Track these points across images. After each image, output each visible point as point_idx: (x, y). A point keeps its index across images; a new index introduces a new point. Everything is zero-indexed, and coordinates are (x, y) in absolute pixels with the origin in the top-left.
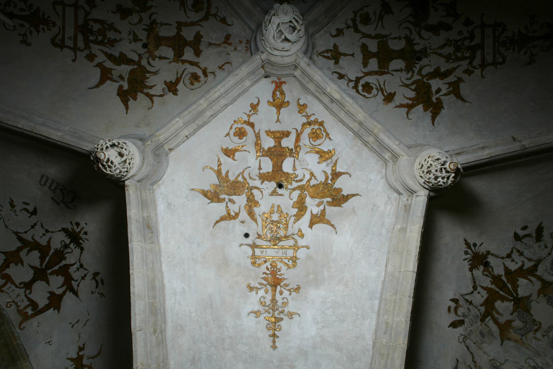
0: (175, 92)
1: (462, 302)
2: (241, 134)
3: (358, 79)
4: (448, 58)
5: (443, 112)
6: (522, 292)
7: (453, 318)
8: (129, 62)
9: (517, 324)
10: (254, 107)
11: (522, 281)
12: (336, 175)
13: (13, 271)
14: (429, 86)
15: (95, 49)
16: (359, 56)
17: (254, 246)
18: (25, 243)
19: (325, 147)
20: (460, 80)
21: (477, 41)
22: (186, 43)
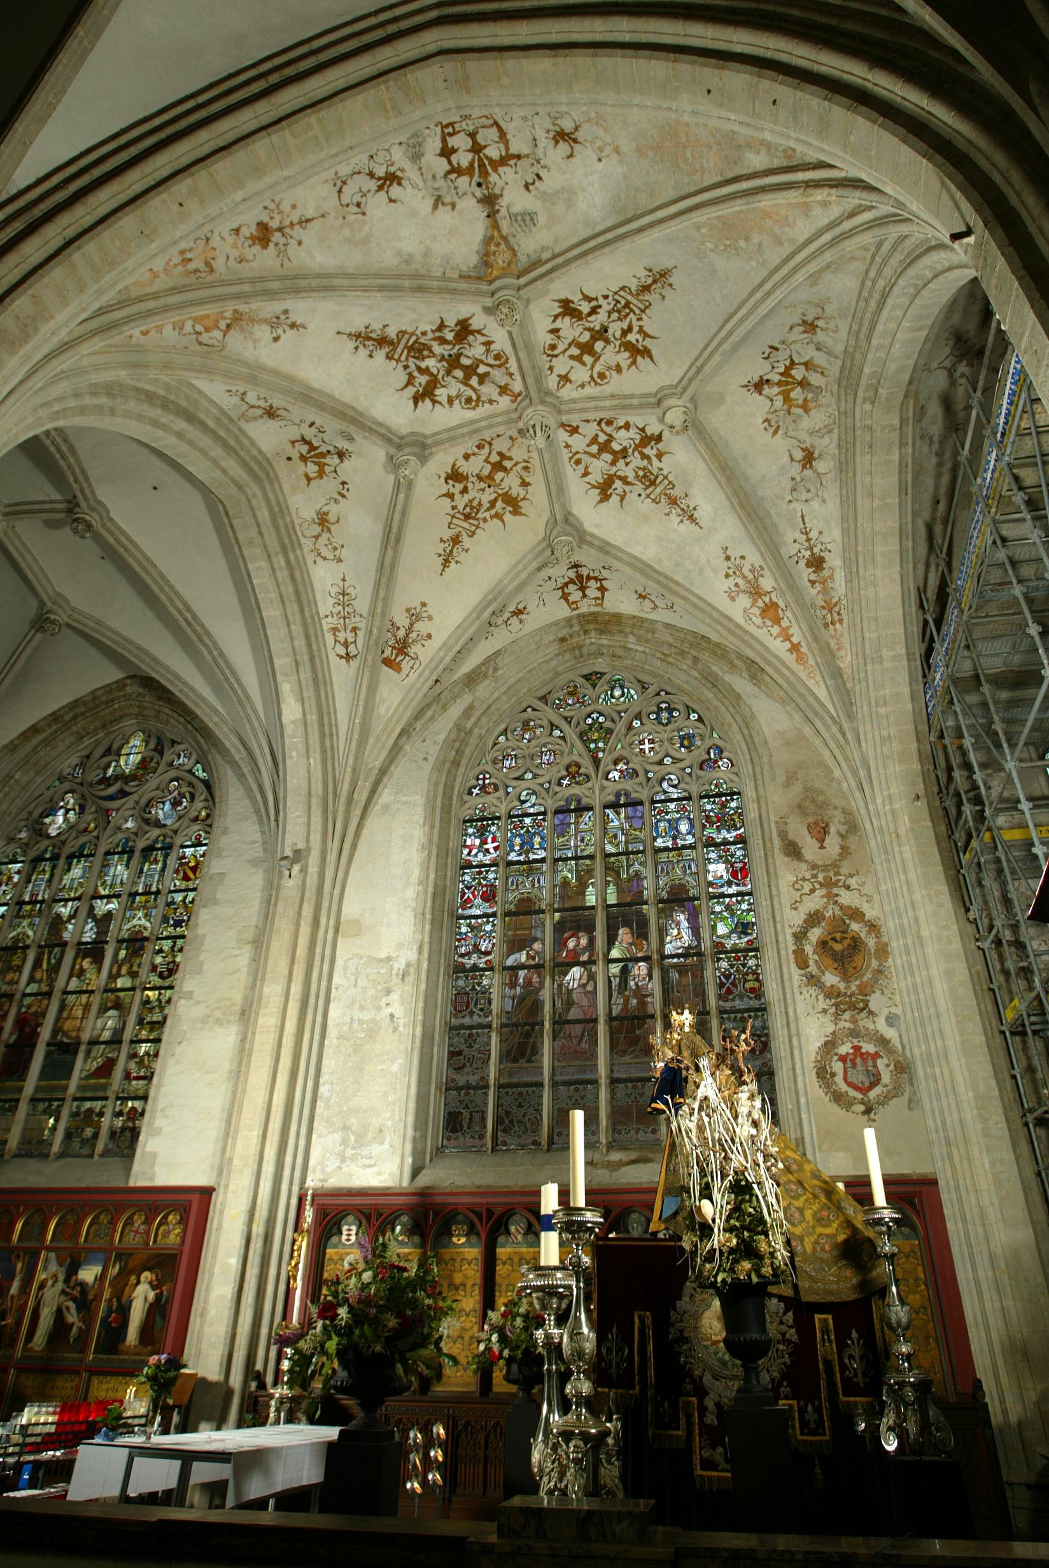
0: (529, 484)
1: (770, 416)
2: (578, 462)
3: (592, 377)
4: (619, 319)
5: (653, 352)
6: (799, 378)
7: (771, 430)
8: (496, 500)
9: (810, 396)
10: (567, 446)
11: (793, 372)
12: (643, 430)
13: (571, 599)
14: (630, 342)
15: (480, 515)
16: (575, 364)
17: (648, 496)
18: (562, 588)
19: (621, 423)
20: (641, 327)
21: (623, 302)
22: (500, 462)
